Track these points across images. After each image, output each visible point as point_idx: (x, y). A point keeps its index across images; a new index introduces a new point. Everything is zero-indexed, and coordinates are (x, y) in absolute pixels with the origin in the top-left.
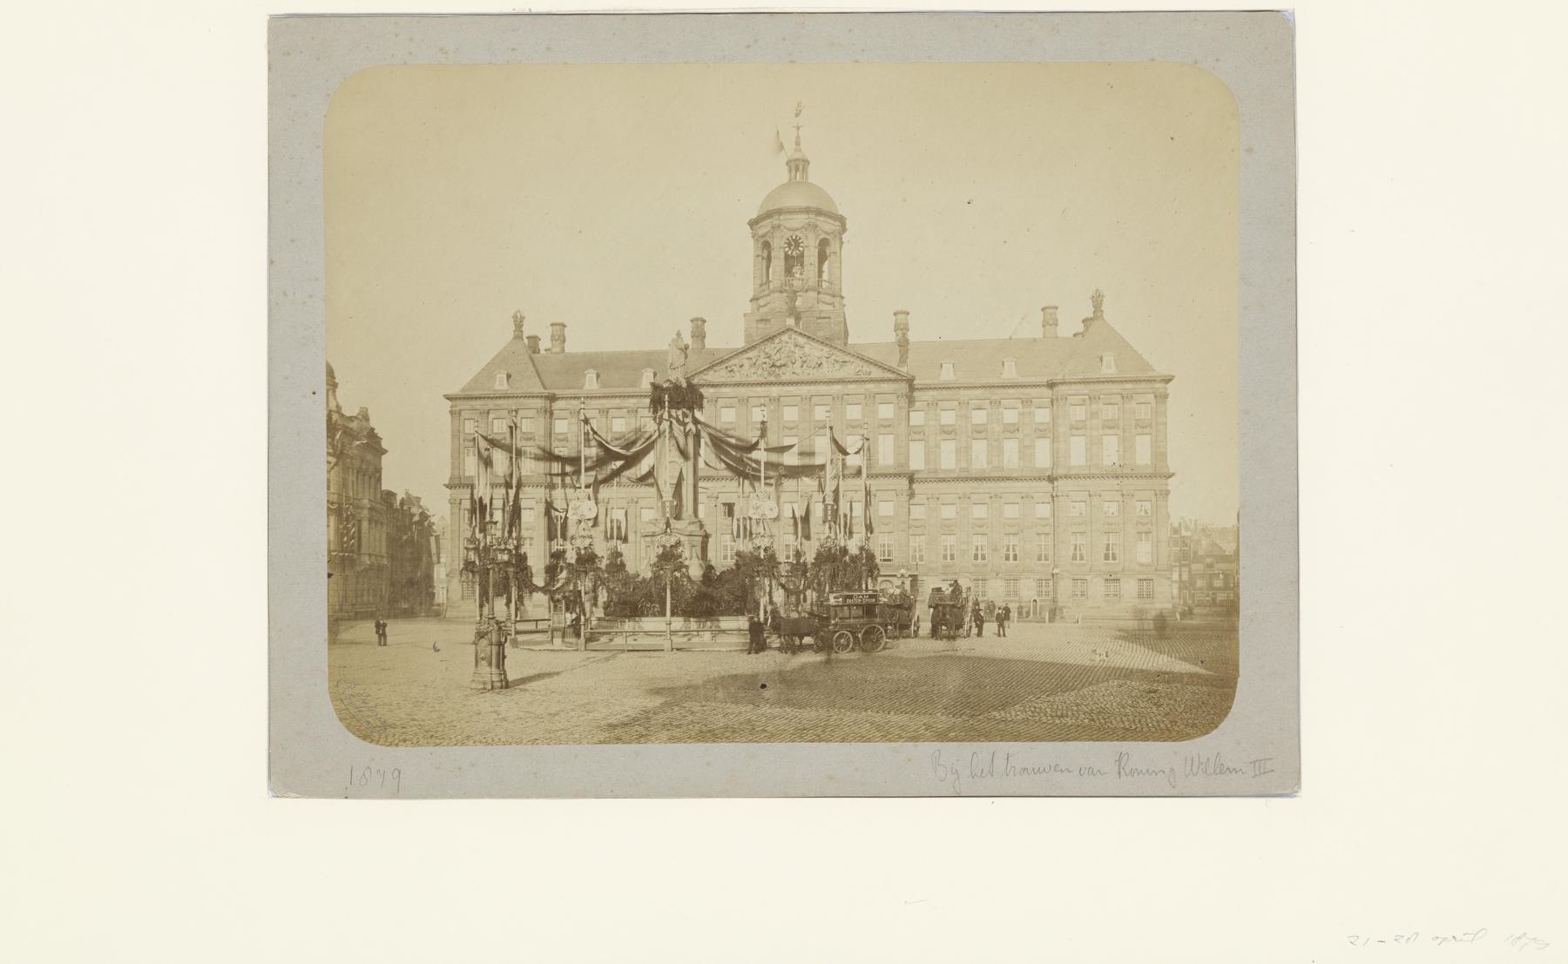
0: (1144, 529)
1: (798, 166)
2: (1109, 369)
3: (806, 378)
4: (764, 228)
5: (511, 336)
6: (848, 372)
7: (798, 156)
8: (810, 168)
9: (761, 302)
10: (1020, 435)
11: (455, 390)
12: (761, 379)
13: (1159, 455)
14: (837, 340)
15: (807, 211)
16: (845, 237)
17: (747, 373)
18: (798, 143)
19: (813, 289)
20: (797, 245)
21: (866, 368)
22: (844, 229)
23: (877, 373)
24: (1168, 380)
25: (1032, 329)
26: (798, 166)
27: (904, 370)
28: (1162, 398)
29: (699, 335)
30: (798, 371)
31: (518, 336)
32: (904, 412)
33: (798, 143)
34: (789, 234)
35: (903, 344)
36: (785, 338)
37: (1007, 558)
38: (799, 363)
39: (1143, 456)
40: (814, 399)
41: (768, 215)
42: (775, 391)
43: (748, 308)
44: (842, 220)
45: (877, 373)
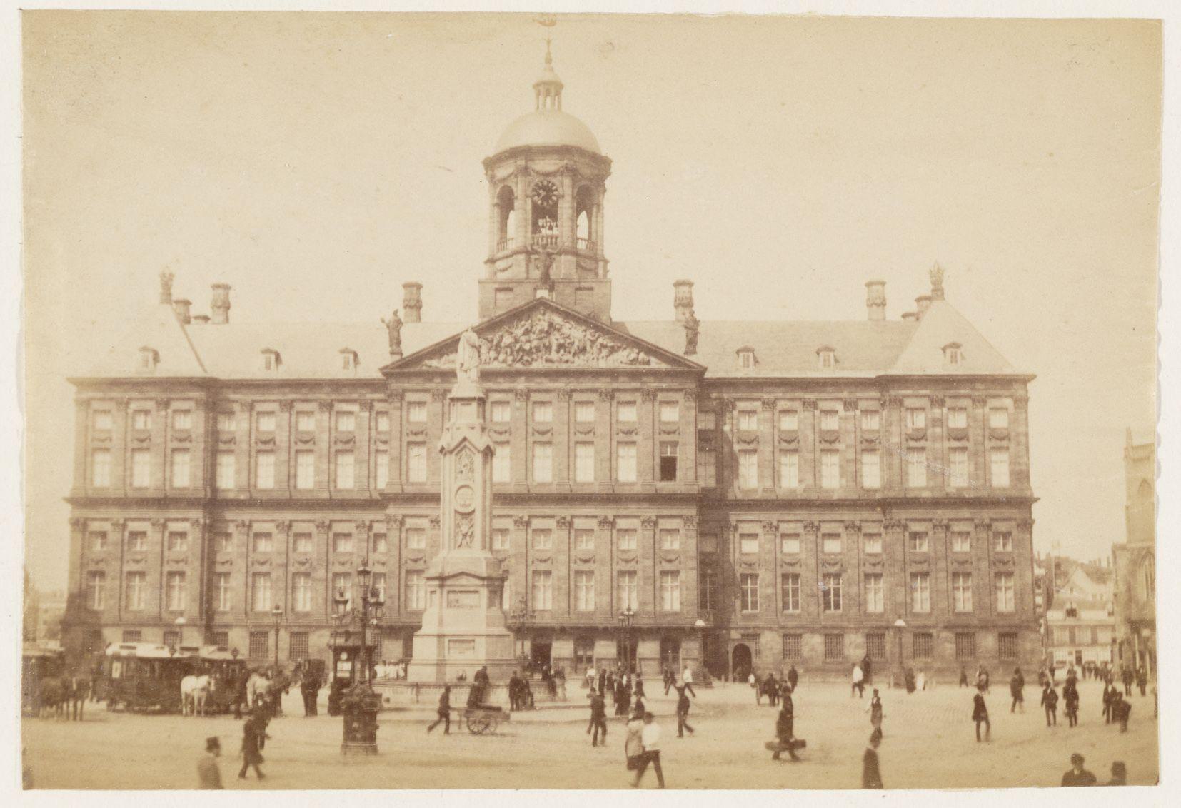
0: (1002, 568)
3: (564, 366)
4: (502, 172)
6: (622, 360)
7: (548, 77)
8: (563, 92)
9: (501, 264)
11: (85, 371)
12: (503, 367)
13: (1021, 475)
15: (562, 151)
16: (607, 183)
18: (549, 61)
19: (566, 252)
20: (548, 190)
21: (642, 356)
22: (608, 174)
23: (655, 364)
24: (1024, 380)
26: (550, 89)
27: (693, 358)
28: (1022, 403)
29: (415, 306)
30: (554, 356)
31: (167, 296)
32: (693, 412)
33: (549, 61)
35: (692, 329)
37: (827, 606)
38: (554, 347)
39: (1000, 477)
40: (576, 397)
41: (514, 153)
42: (521, 384)
43: (484, 272)
45: (655, 364)
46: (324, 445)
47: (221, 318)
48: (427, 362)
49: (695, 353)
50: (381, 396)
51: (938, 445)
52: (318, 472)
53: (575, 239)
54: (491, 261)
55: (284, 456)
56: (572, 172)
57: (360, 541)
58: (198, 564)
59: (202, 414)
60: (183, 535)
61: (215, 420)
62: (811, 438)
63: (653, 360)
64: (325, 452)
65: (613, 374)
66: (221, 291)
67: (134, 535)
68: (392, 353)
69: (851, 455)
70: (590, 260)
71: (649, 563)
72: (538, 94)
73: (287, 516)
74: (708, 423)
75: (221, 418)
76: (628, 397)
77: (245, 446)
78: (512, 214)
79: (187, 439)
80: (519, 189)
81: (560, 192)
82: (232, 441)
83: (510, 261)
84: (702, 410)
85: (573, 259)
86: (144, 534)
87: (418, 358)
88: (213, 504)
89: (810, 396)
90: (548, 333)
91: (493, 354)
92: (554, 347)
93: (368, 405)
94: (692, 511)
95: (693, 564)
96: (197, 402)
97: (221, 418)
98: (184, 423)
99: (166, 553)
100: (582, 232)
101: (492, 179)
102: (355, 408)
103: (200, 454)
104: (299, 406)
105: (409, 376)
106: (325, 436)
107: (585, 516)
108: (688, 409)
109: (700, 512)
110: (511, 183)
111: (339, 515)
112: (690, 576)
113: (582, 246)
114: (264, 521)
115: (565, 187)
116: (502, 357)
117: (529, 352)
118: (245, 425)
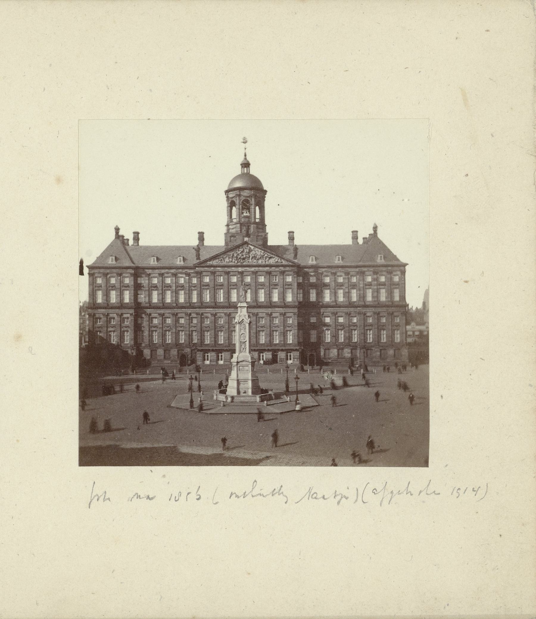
1: (246, 165)
2: (380, 260)
4: (231, 195)
5: (114, 238)
6: (272, 261)
8: (251, 167)
9: (230, 227)
10: (344, 287)
14: (264, 245)
17: (227, 261)
18: (245, 155)
20: (248, 201)
21: (279, 260)
23: (284, 263)
25: (349, 241)
27: (296, 261)
31: (118, 236)
33: (245, 155)
34: (243, 198)
36: (245, 246)
38: (251, 258)
42: (240, 269)
44: (266, 191)
46: (174, 288)
47: (137, 244)
48: (209, 262)
49: (296, 259)
50: (192, 271)
51: (376, 287)
52: (172, 297)
53: (255, 218)
54: (228, 225)
55: (161, 292)
56: (255, 197)
57: (186, 319)
58: (133, 328)
59: (132, 278)
60: (128, 318)
61: (137, 280)
62: (334, 285)
63: (283, 261)
64: (174, 290)
65: (271, 266)
66: (136, 234)
67: (111, 318)
68: (197, 259)
69: (347, 291)
70: (262, 225)
71: (282, 328)
72: (242, 167)
73: (162, 311)
74: (301, 280)
75: (139, 279)
76: (275, 274)
77: (147, 289)
78: (234, 208)
79: (128, 286)
80: (237, 202)
81: (251, 203)
82: (143, 287)
83: (234, 226)
84: (298, 276)
85: (255, 226)
86: (114, 318)
87: (206, 261)
88: (138, 309)
89: (334, 271)
90: (249, 253)
91: (230, 260)
92: (251, 258)
93: (188, 275)
94: (296, 310)
95: (296, 328)
96: (131, 274)
97: (139, 279)
98: (127, 281)
99: (122, 324)
100: (258, 216)
101: (227, 197)
102: (184, 276)
103: (133, 292)
104: (166, 275)
105: (203, 267)
106: (174, 285)
107: (262, 312)
108: (295, 277)
109: (298, 311)
110: (234, 199)
111: (179, 311)
112: (295, 331)
113: (257, 221)
114: (155, 313)
115: (253, 201)
116: (234, 260)
117: (244, 259)
118: (147, 281)
